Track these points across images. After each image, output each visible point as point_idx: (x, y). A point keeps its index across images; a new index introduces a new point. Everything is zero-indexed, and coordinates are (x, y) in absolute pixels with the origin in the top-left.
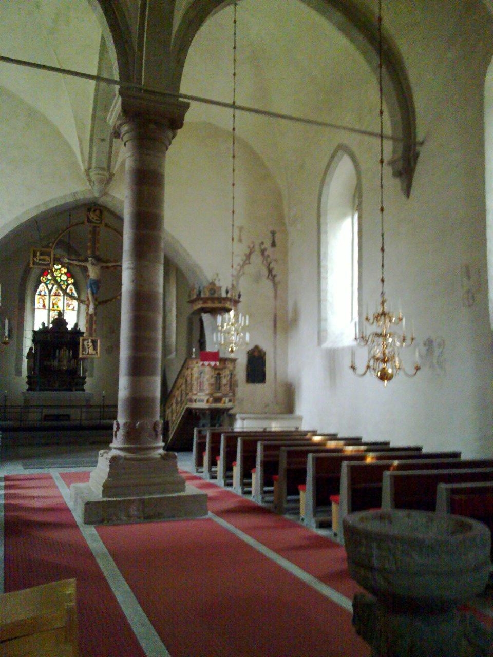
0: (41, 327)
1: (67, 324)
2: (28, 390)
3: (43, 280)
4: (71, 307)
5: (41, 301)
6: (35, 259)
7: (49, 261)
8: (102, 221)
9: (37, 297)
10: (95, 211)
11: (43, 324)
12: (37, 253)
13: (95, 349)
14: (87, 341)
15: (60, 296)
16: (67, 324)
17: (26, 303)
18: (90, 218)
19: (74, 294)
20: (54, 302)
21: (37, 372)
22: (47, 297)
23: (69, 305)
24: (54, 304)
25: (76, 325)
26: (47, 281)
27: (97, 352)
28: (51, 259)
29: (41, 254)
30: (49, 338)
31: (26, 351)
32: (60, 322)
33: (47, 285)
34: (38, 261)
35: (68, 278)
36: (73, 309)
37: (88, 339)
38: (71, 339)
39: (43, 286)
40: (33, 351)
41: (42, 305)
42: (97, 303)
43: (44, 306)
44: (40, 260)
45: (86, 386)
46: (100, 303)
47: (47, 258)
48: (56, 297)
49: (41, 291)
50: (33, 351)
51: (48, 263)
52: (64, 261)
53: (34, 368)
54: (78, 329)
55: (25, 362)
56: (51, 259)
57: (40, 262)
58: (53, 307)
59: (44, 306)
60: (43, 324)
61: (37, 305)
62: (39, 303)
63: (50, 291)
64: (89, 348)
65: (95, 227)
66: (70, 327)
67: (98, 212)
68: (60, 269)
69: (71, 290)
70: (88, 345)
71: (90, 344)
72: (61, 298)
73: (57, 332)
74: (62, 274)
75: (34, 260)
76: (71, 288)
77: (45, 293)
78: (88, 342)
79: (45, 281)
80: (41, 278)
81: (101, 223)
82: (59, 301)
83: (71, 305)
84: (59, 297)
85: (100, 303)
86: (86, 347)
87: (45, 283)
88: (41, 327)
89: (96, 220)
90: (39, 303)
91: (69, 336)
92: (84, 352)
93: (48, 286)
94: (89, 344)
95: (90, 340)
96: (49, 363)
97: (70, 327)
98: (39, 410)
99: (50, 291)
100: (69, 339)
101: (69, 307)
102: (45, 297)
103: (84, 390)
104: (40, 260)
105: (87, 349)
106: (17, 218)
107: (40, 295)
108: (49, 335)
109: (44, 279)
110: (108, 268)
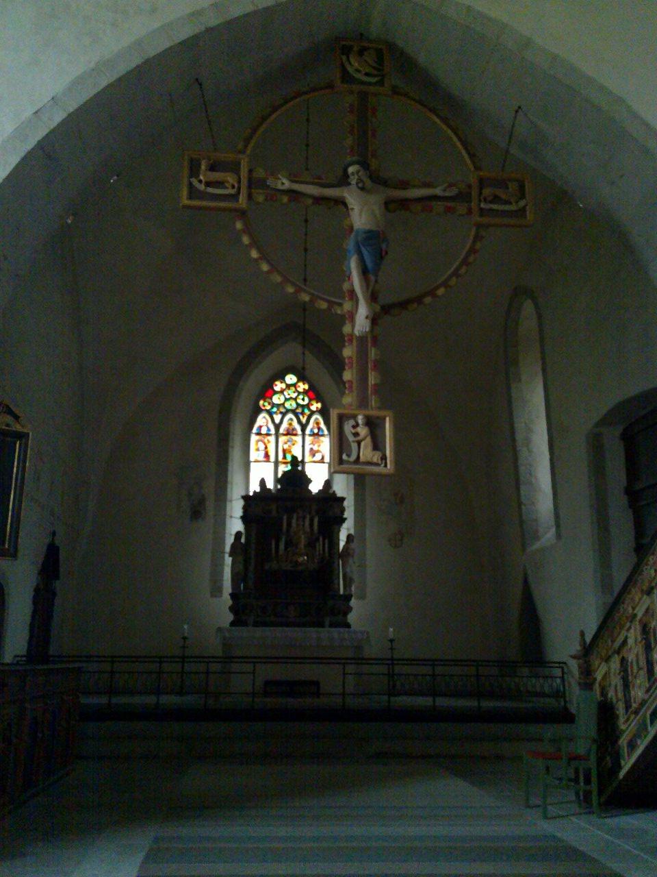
0: (258, 490)
1: (309, 481)
2: (233, 624)
3: (264, 406)
4: (318, 457)
5: (261, 446)
6: (195, 182)
7: (233, 187)
8: (383, 76)
9: (254, 438)
10: (361, 52)
11: (263, 483)
12: (199, 165)
13: (377, 445)
14: (352, 422)
15: (296, 435)
16: (309, 481)
17: (233, 447)
18: (350, 69)
19: (323, 431)
20: (286, 447)
22: (272, 439)
23: (313, 453)
24: (284, 451)
25: (328, 484)
26: (272, 408)
27: (384, 458)
28: (239, 182)
29: (212, 168)
31: (230, 540)
32: (295, 478)
33: (270, 414)
34: (202, 187)
35: (310, 400)
36: (322, 461)
37: (354, 417)
39: (264, 417)
40: (243, 540)
41: (262, 453)
42: (378, 308)
43: (267, 456)
44: (208, 184)
45: (351, 618)
46: (386, 309)
47: (230, 178)
48: (289, 436)
49: (260, 427)
50: (243, 540)
51: (232, 191)
52: (280, 187)
53: (246, 575)
54: (331, 491)
55: (228, 560)
56: (239, 182)
57: (210, 190)
58: (284, 457)
59: (267, 456)
60: (263, 483)
61: (254, 455)
62: (258, 450)
63: (277, 427)
64: (359, 443)
65: (363, 96)
66: (315, 487)
67: (370, 57)
68: (295, 385)
69: (318, 424)
70: (356, 434)
71: (363, 431)
72: (299, 439)
74: (299, 393)
75: (191, 184)
76: (317, 419)
77: (269, 430)
78: (356, 425)
79: (268, 407)
80: (261, 402)
81: (381, 83)
82: (294, 444)
83: (318, 451)
84: (294, 438)
85: (386, 309)
86: (351, 438)
88: (258, 490)
89: (367, 74)
90: (258, 450)
92: (344, 457)
93: (275, 416)
94: (359, 430)
95: (360, 419)
97: (315, 487)
98: (249, 667)
99: (277, 427)
101: (314, 455)
102: (269, 438)
103: (348, 626)
104: (208, 184)
105: (354, 446)
106: (138, 43)
107: (259, 434)
108: (274, 507)
110: (404, 204)
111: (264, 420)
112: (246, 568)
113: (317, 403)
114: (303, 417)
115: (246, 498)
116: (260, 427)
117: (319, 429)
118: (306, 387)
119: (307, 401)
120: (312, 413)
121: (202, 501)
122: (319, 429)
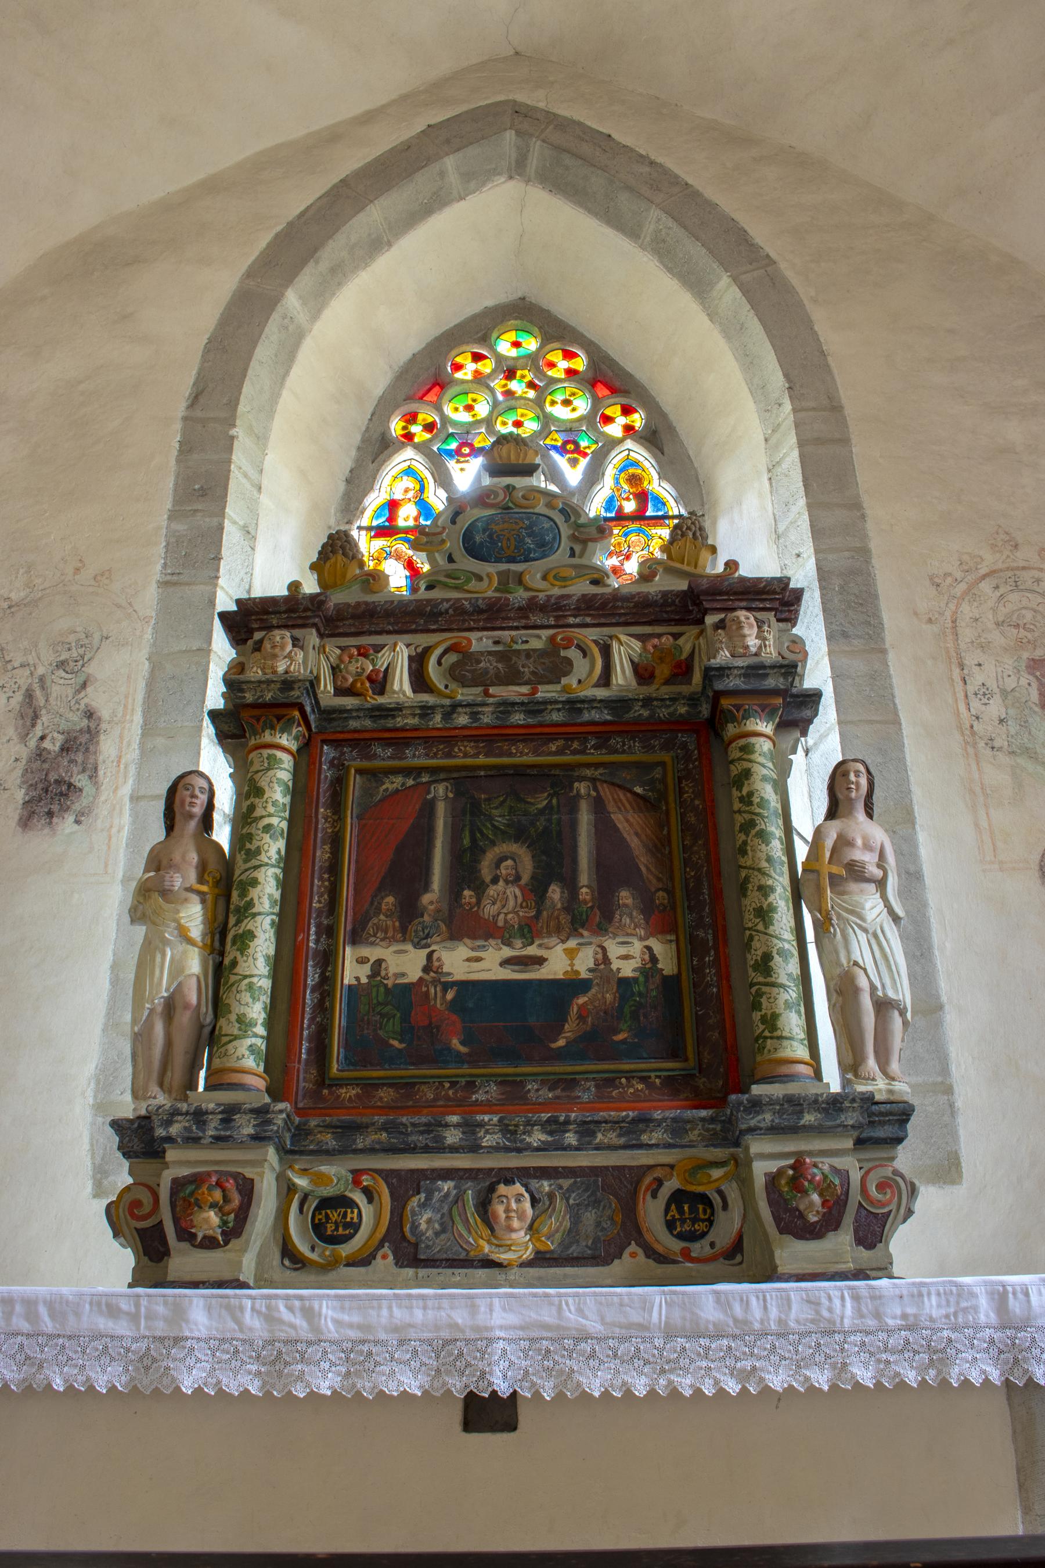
19: (660, 502)
21: (248, 1053)
30: (401, 684)
38: (643, 673)
39: (409, 472)
49: (393, 505)
68: (533, 360)
69: (634, 480)
73: (491, 614)
87: (423, 448)
91: (626, 649)
93: (452, 465)
96: (405, 963)
100: (623, 676)
108: (397, 657)
109: (416, 429)
111: (409, 482)
112: (221, 972)
113: (627, 411)
114: (574, 463)
115: (248, 622)
116: (393, 505)
117: (643, 497)
118: (580, 364)
119: (582, 405)
120: (612, 443)
121: (81, 742)
122: (643, 497)
